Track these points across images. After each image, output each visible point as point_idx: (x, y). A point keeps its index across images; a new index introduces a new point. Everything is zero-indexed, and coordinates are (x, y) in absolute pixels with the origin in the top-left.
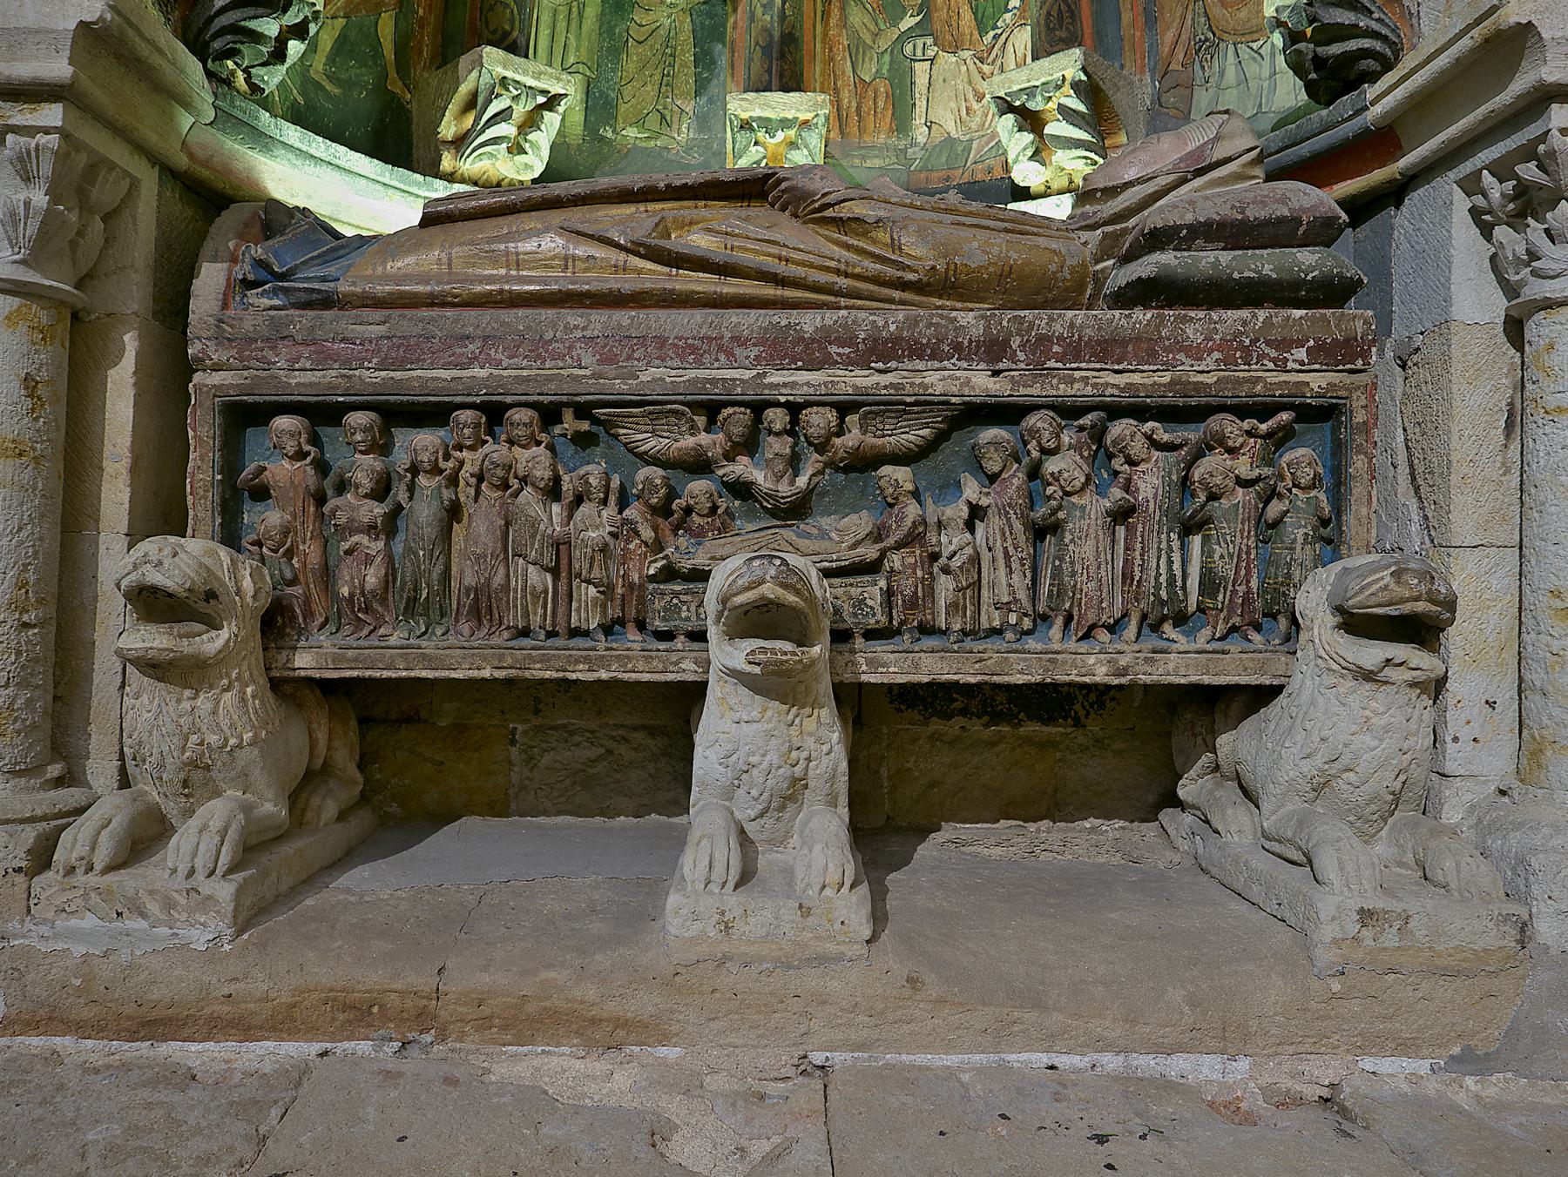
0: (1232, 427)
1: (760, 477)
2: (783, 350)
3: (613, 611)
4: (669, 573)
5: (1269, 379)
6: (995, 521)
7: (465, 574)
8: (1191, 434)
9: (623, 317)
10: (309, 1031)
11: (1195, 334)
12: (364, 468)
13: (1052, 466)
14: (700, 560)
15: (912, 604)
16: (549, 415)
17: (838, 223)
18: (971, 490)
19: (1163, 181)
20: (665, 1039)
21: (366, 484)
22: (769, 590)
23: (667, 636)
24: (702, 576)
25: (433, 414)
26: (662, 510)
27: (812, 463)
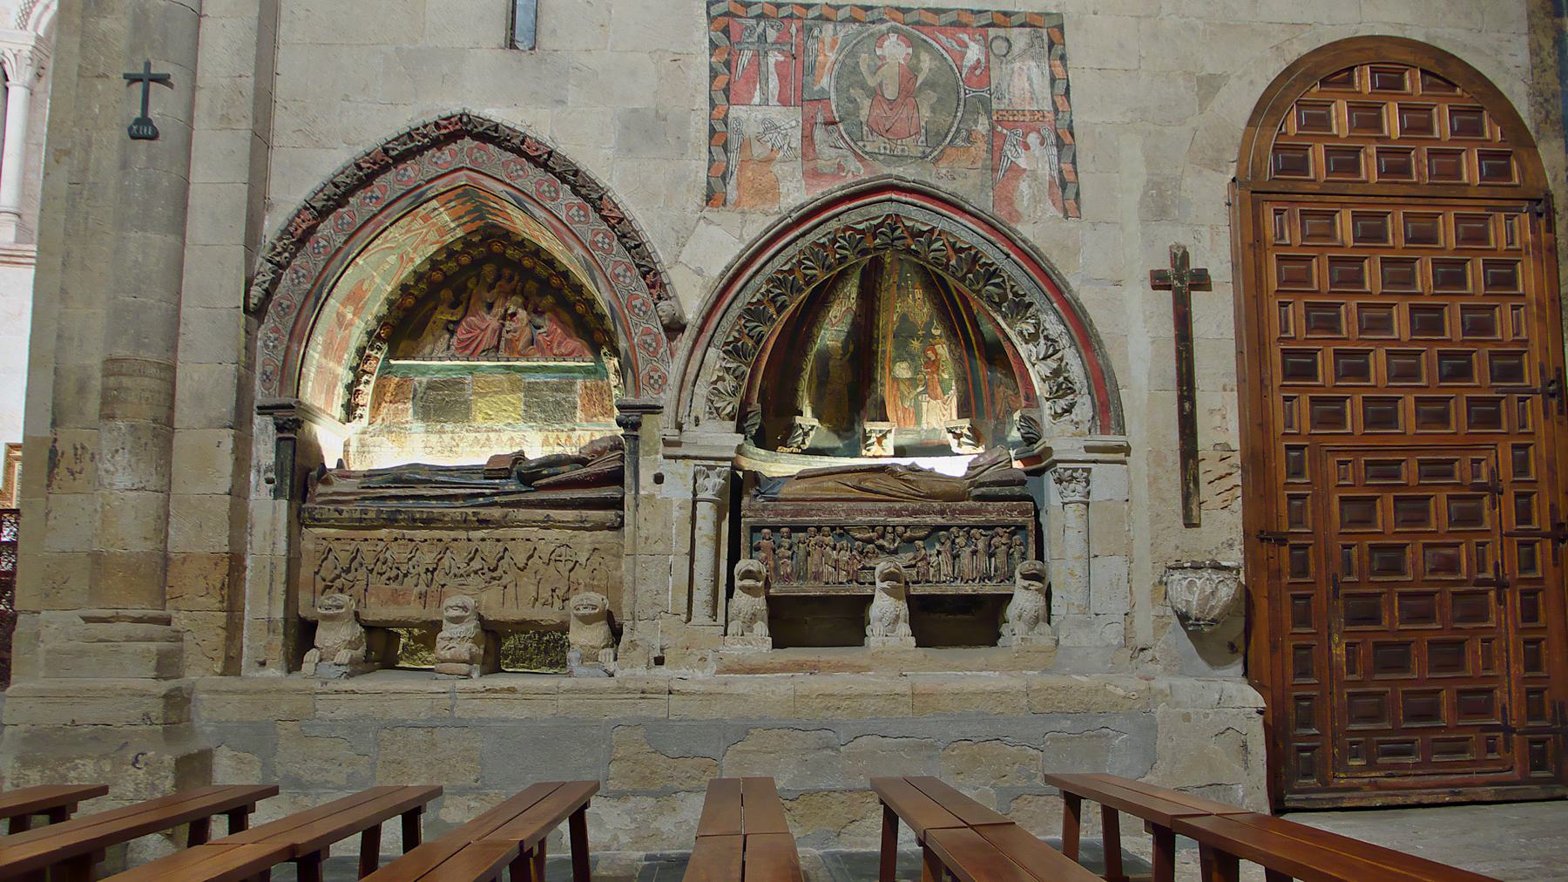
0: (1000, 530)
1: (885, 543)
2: (891, 512)
3: (850, 578)
4: (864, 568)
5: (1008, 519)
6: (943, 554)
7: (812, 568)
8: (989, 532)
9: (852, 504)
10: (790, 671)
11: (990, 508)
12: (786, 542)
13: (957, 540)
14: (872, 565)
15: (923, 574)
16: (833, 529)
17: (903, 480)
18: (938, 546)
19: (986, 467)
20: (870, 670)
21: (787, 546)
22: (892, 569)
23: (864, 584)
24: (874, 569)
25: (804, 529)
26: (861, 553)
27: (898, 540)
